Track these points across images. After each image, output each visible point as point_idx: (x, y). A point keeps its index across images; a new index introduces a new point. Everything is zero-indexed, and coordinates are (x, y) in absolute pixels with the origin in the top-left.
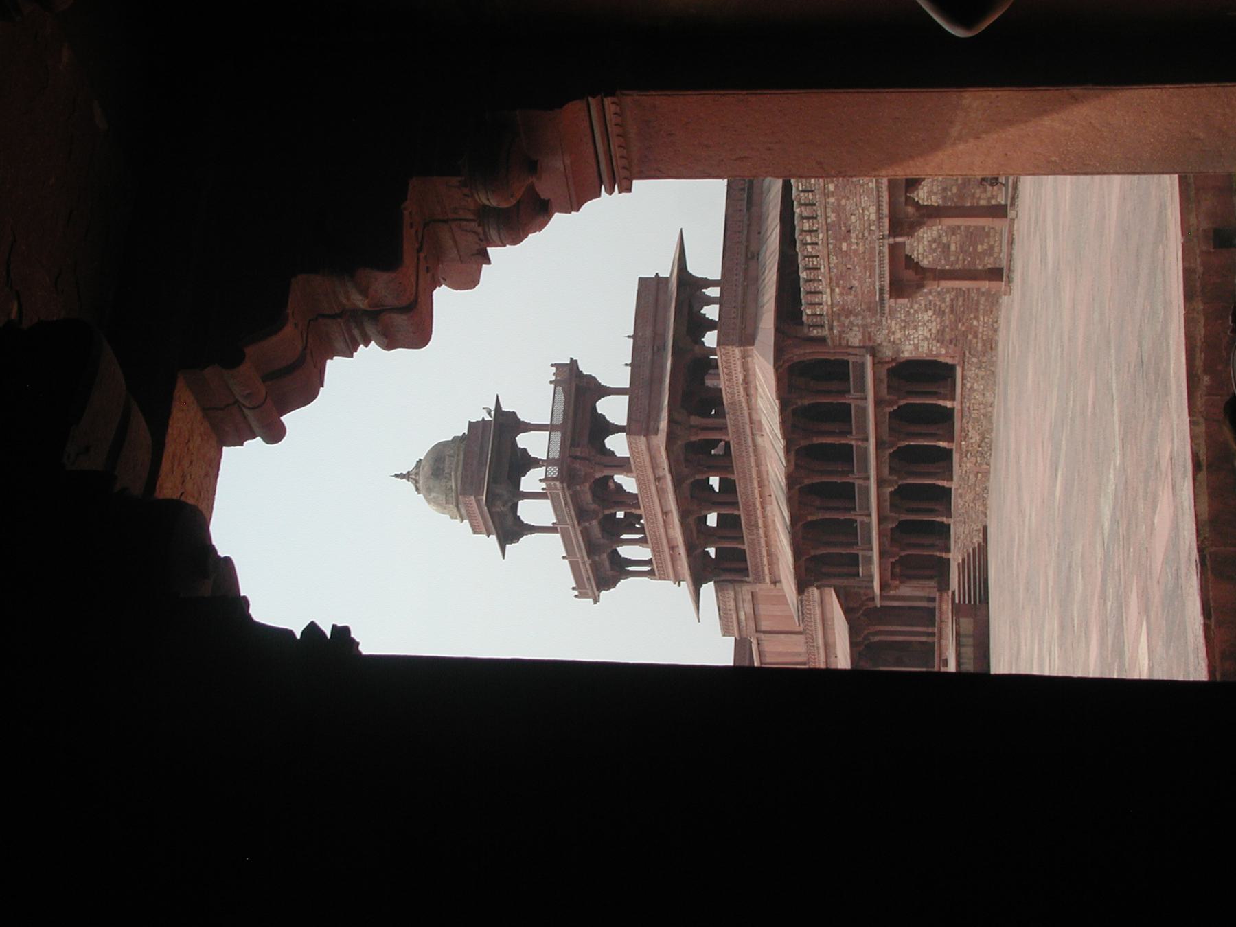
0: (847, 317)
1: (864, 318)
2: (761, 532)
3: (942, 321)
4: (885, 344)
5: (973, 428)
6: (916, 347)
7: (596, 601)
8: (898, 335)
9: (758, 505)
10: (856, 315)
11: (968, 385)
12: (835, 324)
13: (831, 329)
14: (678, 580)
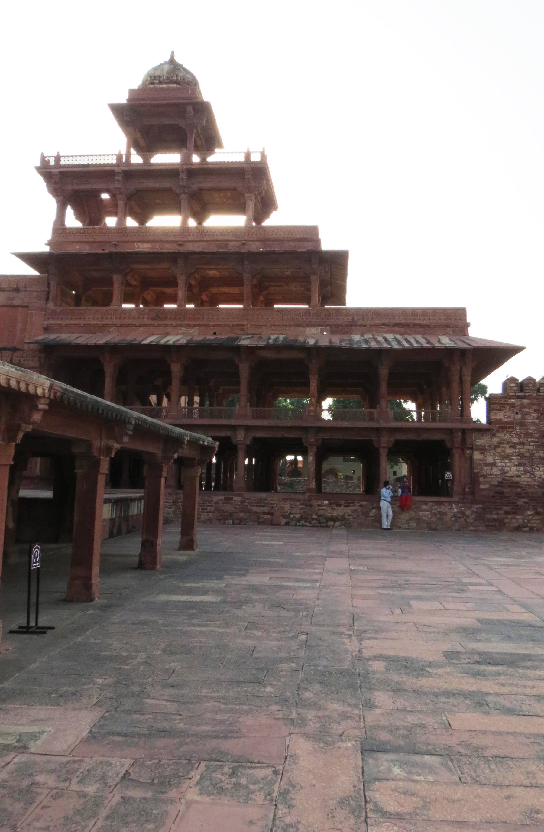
0: (535, 411)
1: (534, 424)
2: (146, 321)
3: (533, 486)
4: (495, 440)
5: (354, 511)
6: (494, 464)
7: (37, 168)
8: (509, 451)
9: (197, 323)
10: (538, 418)
11: (424, 507)
12: (526, 401)
13: (519, 397)
14: (50, 243)
